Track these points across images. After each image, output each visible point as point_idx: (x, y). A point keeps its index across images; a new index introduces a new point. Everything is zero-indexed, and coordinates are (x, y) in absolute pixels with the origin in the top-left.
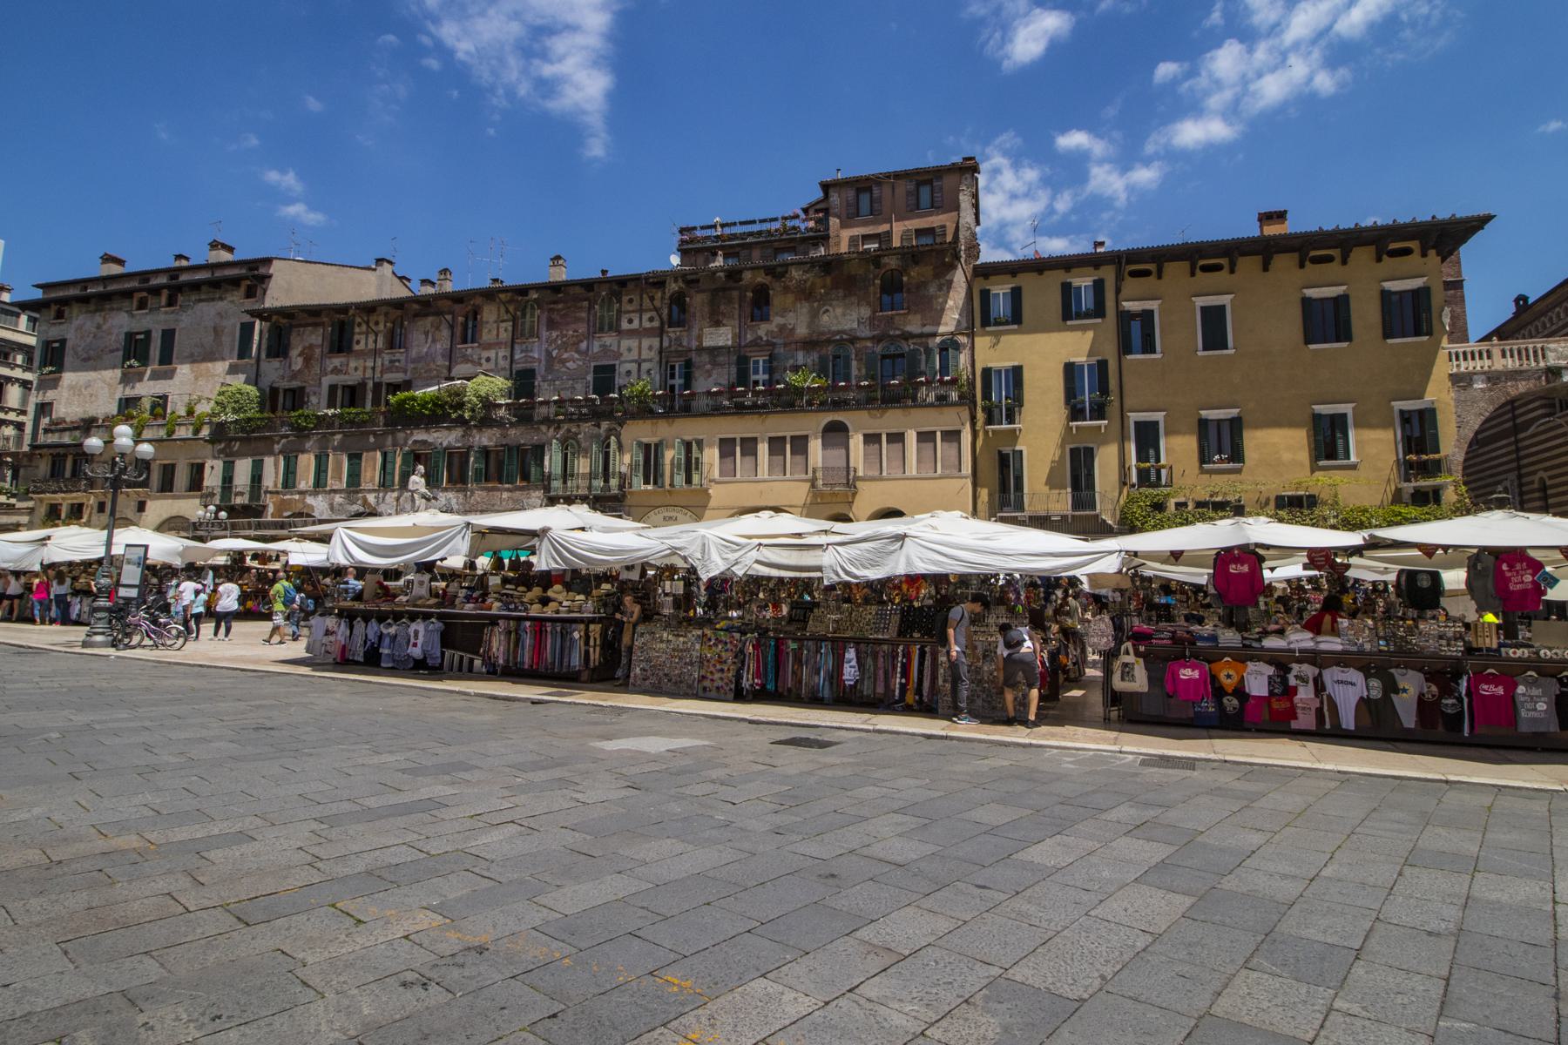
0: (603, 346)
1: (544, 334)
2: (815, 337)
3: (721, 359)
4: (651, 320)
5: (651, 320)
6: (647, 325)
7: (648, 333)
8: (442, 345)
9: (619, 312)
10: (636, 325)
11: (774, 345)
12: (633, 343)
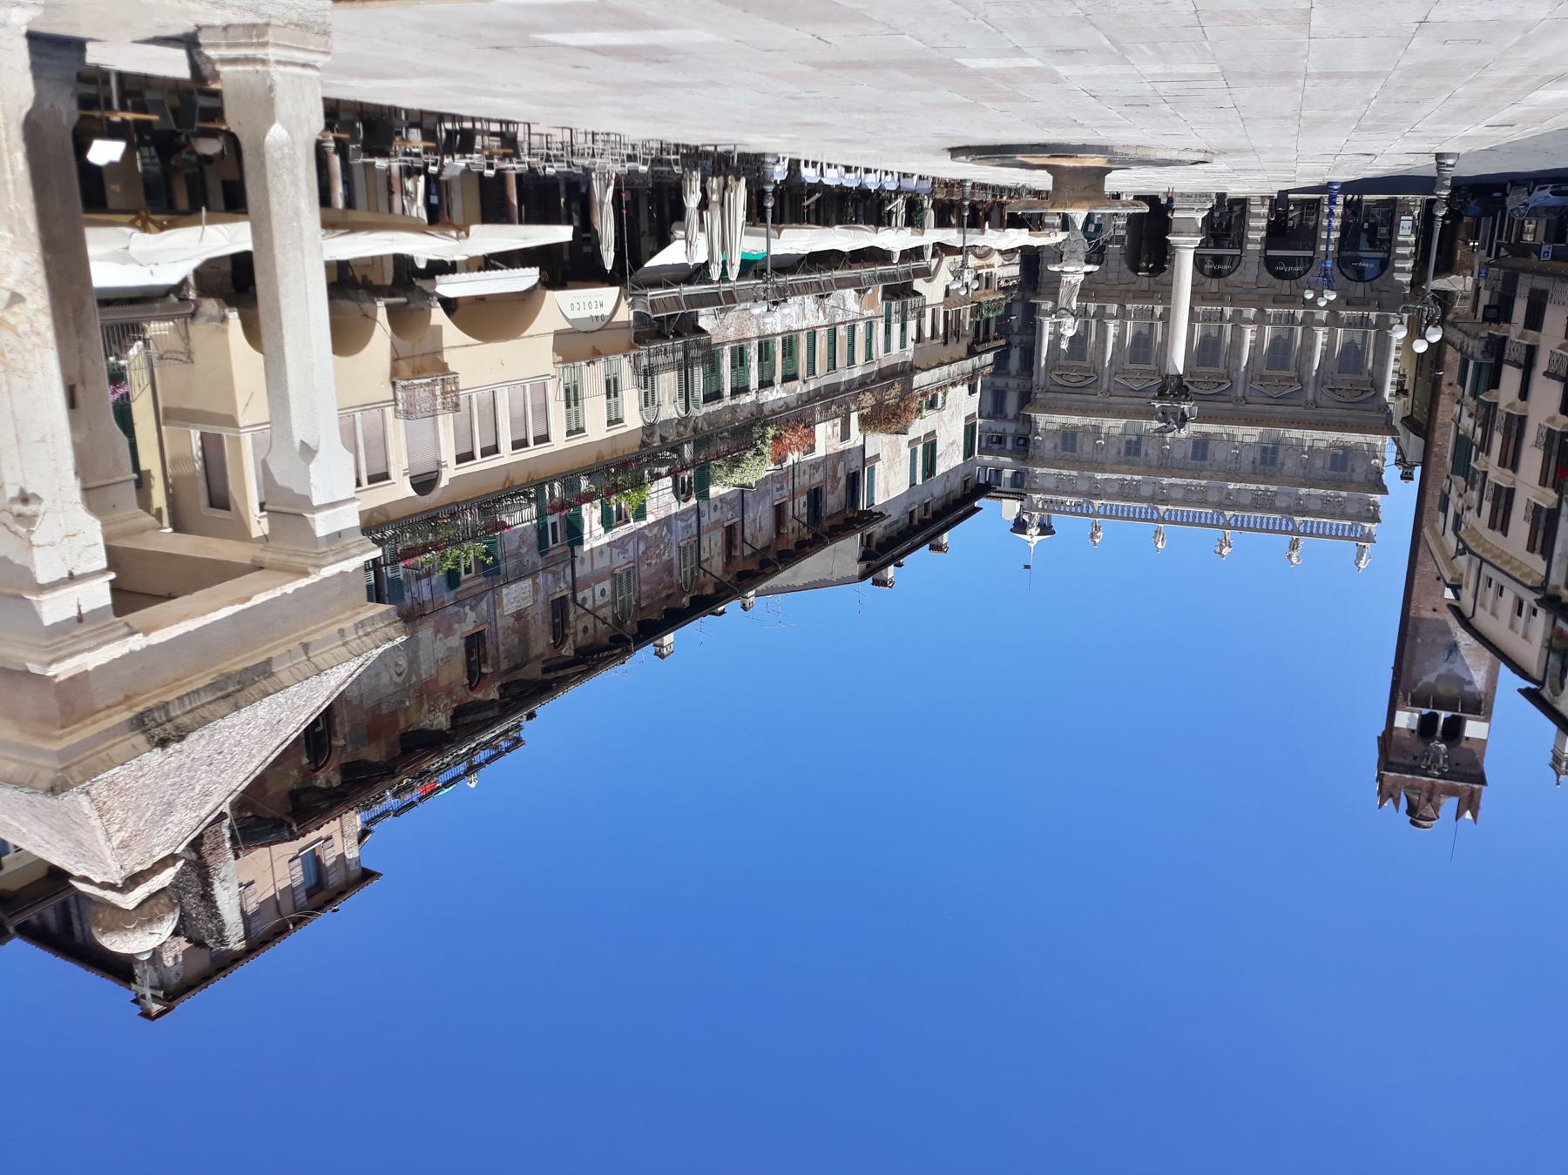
1: (674, 554)
5: (584, 599)
6: (587, 593)
8: (749, 516)
11: (459, 602)
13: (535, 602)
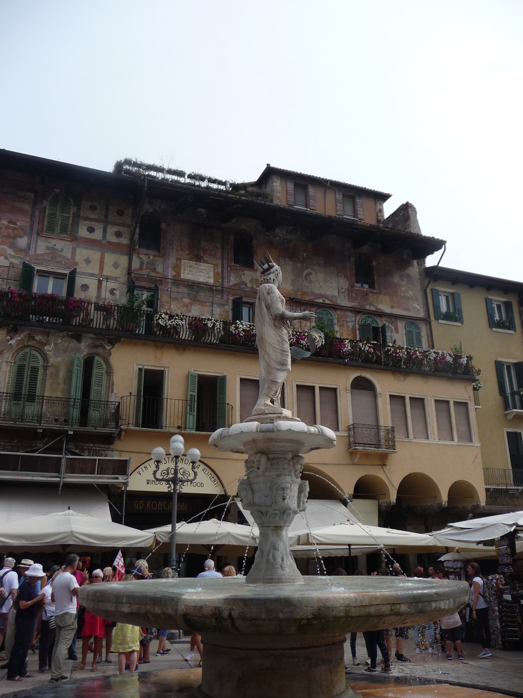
0: (53, 249)
2: (299, 297)
3: (202, 295)
4: (118, 235)
6: (114, 240)
7: (114, 248)
9: (77, 216)
10: (98, 235)
12: (95, 255)
13: (179, 259)
